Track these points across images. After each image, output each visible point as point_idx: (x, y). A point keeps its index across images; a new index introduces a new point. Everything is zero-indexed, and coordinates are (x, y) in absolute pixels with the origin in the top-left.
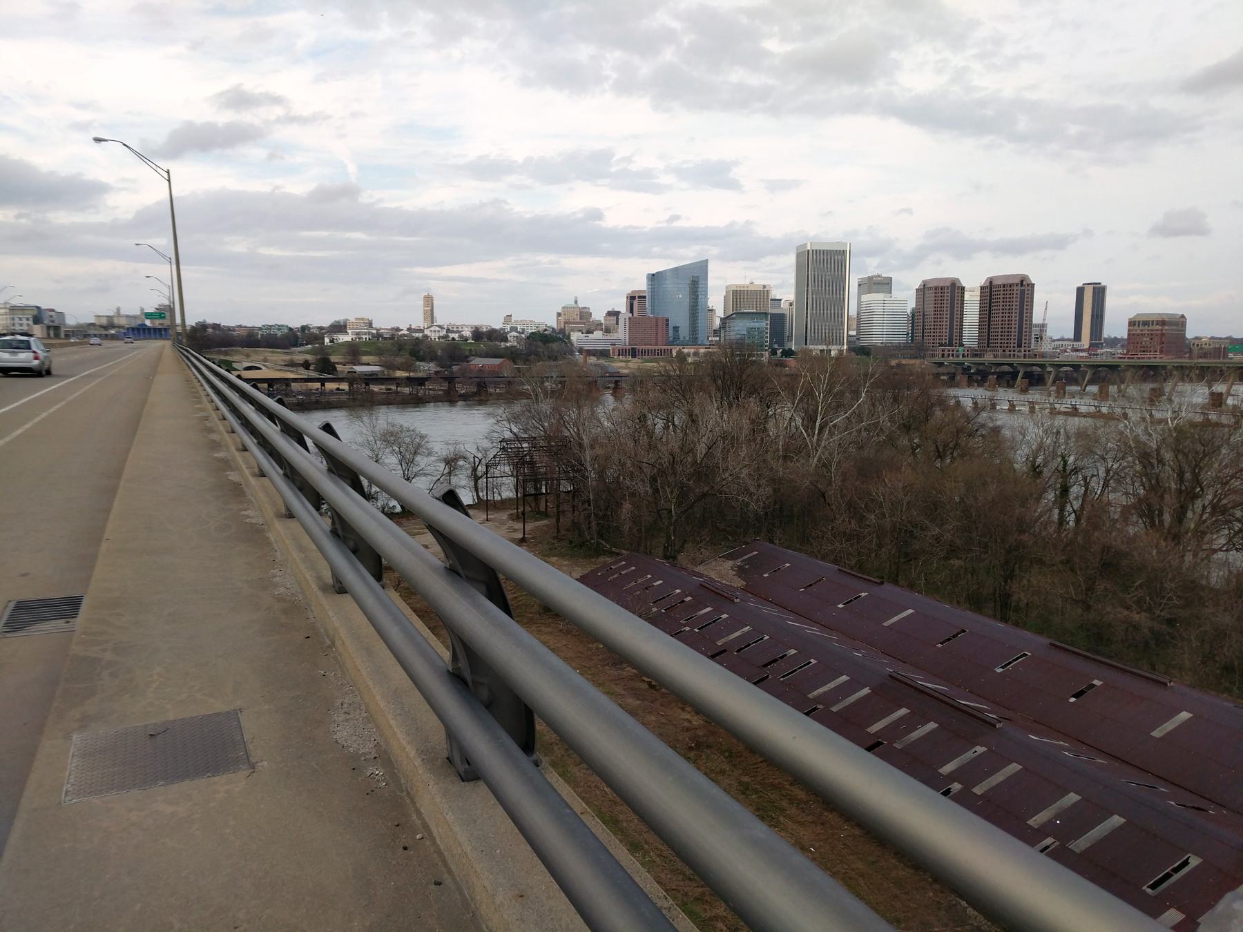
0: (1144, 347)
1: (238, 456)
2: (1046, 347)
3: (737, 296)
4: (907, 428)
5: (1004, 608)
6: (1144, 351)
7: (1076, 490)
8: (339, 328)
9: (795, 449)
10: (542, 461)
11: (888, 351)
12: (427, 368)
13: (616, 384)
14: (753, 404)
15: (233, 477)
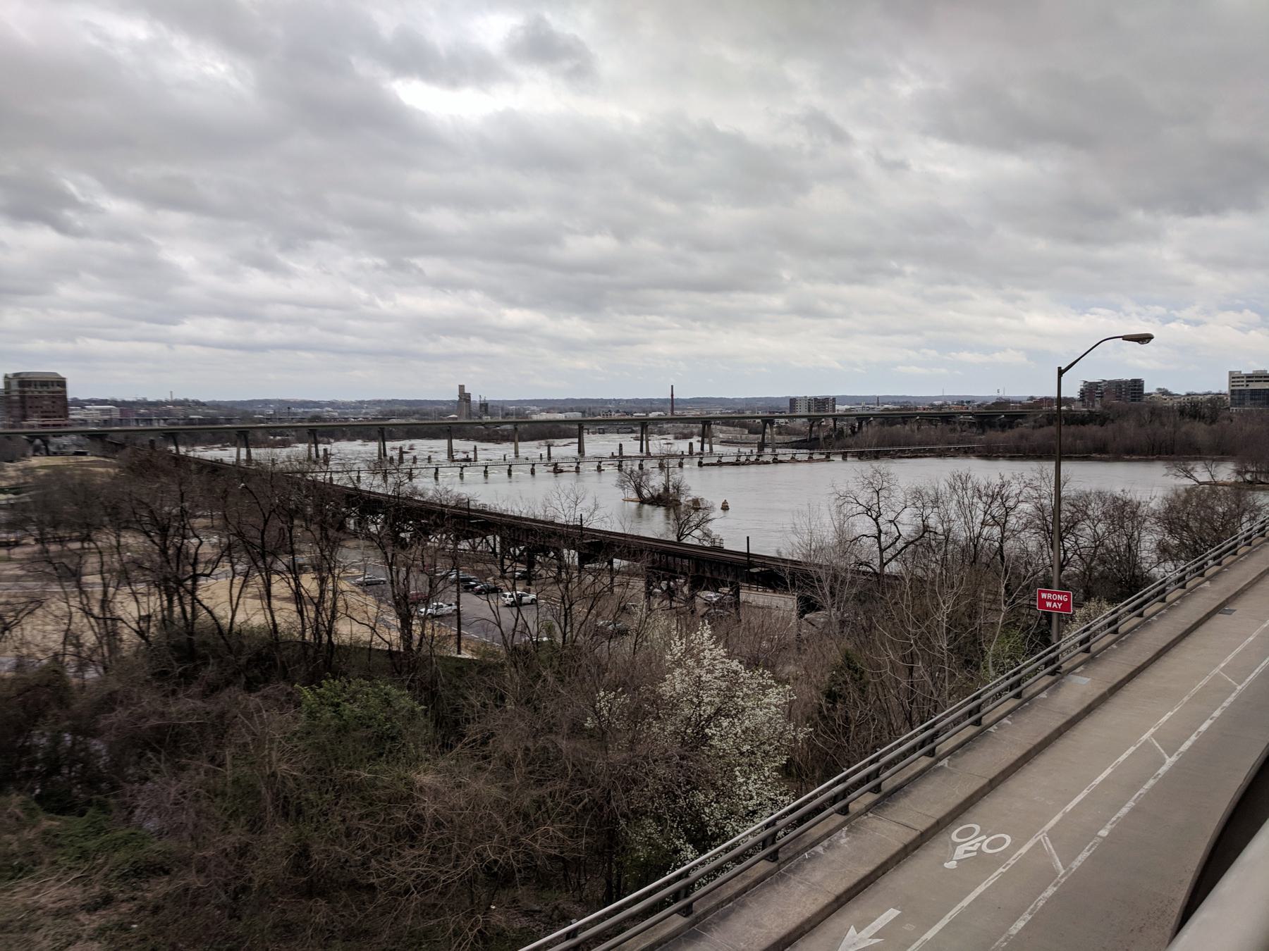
0: (46, 412)
6: (46, 417)
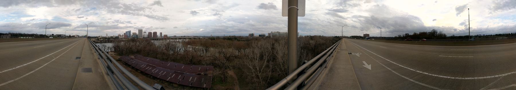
1: (91, 47)
2: (158, 37)
3: (133, 33)
4: (148, 44)
5: (156, 58)
7: (161, 48)
8: (99, 36)
9: (139, 46)
10: (116, 48)
11: (146, 38)
12: (106, 40)
13: (123, 41)
14: (135, 42)
15: (91, 49)
